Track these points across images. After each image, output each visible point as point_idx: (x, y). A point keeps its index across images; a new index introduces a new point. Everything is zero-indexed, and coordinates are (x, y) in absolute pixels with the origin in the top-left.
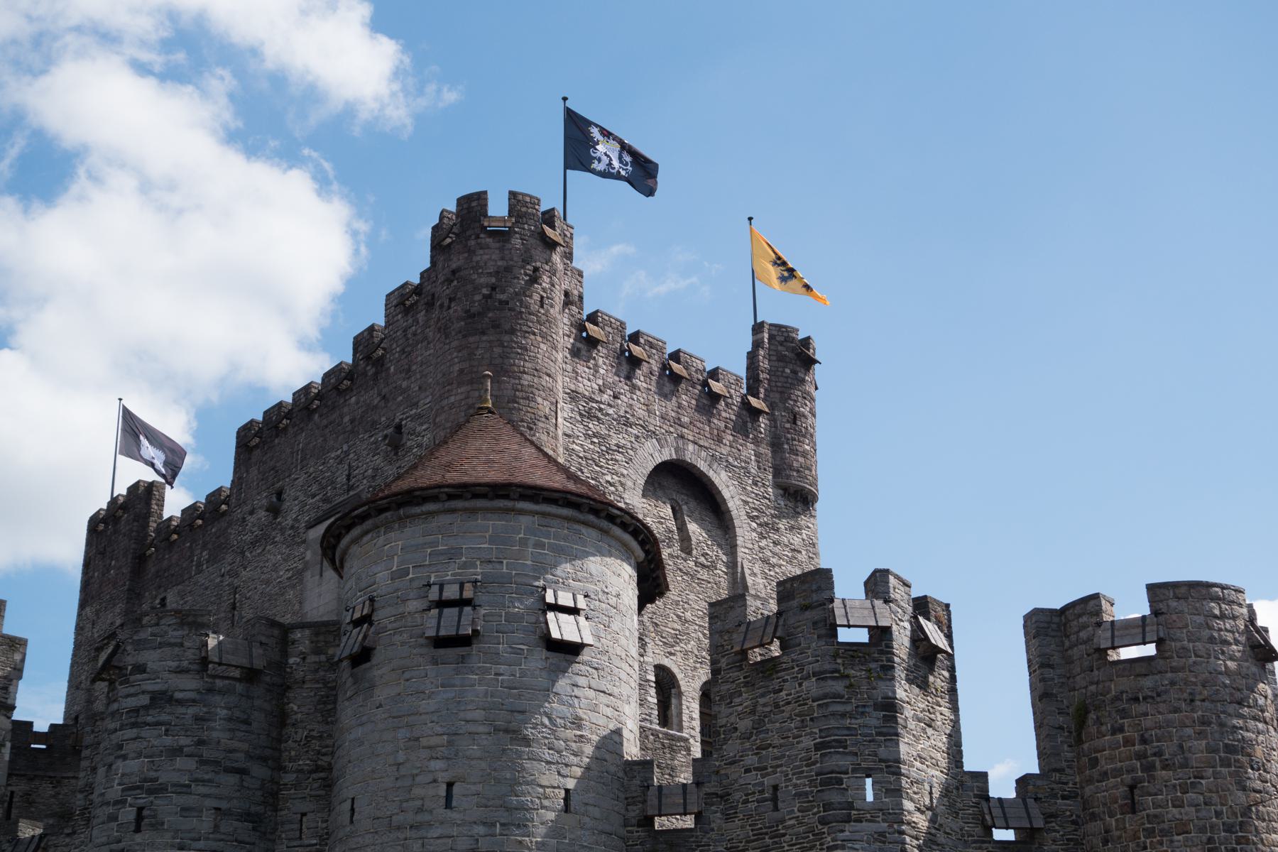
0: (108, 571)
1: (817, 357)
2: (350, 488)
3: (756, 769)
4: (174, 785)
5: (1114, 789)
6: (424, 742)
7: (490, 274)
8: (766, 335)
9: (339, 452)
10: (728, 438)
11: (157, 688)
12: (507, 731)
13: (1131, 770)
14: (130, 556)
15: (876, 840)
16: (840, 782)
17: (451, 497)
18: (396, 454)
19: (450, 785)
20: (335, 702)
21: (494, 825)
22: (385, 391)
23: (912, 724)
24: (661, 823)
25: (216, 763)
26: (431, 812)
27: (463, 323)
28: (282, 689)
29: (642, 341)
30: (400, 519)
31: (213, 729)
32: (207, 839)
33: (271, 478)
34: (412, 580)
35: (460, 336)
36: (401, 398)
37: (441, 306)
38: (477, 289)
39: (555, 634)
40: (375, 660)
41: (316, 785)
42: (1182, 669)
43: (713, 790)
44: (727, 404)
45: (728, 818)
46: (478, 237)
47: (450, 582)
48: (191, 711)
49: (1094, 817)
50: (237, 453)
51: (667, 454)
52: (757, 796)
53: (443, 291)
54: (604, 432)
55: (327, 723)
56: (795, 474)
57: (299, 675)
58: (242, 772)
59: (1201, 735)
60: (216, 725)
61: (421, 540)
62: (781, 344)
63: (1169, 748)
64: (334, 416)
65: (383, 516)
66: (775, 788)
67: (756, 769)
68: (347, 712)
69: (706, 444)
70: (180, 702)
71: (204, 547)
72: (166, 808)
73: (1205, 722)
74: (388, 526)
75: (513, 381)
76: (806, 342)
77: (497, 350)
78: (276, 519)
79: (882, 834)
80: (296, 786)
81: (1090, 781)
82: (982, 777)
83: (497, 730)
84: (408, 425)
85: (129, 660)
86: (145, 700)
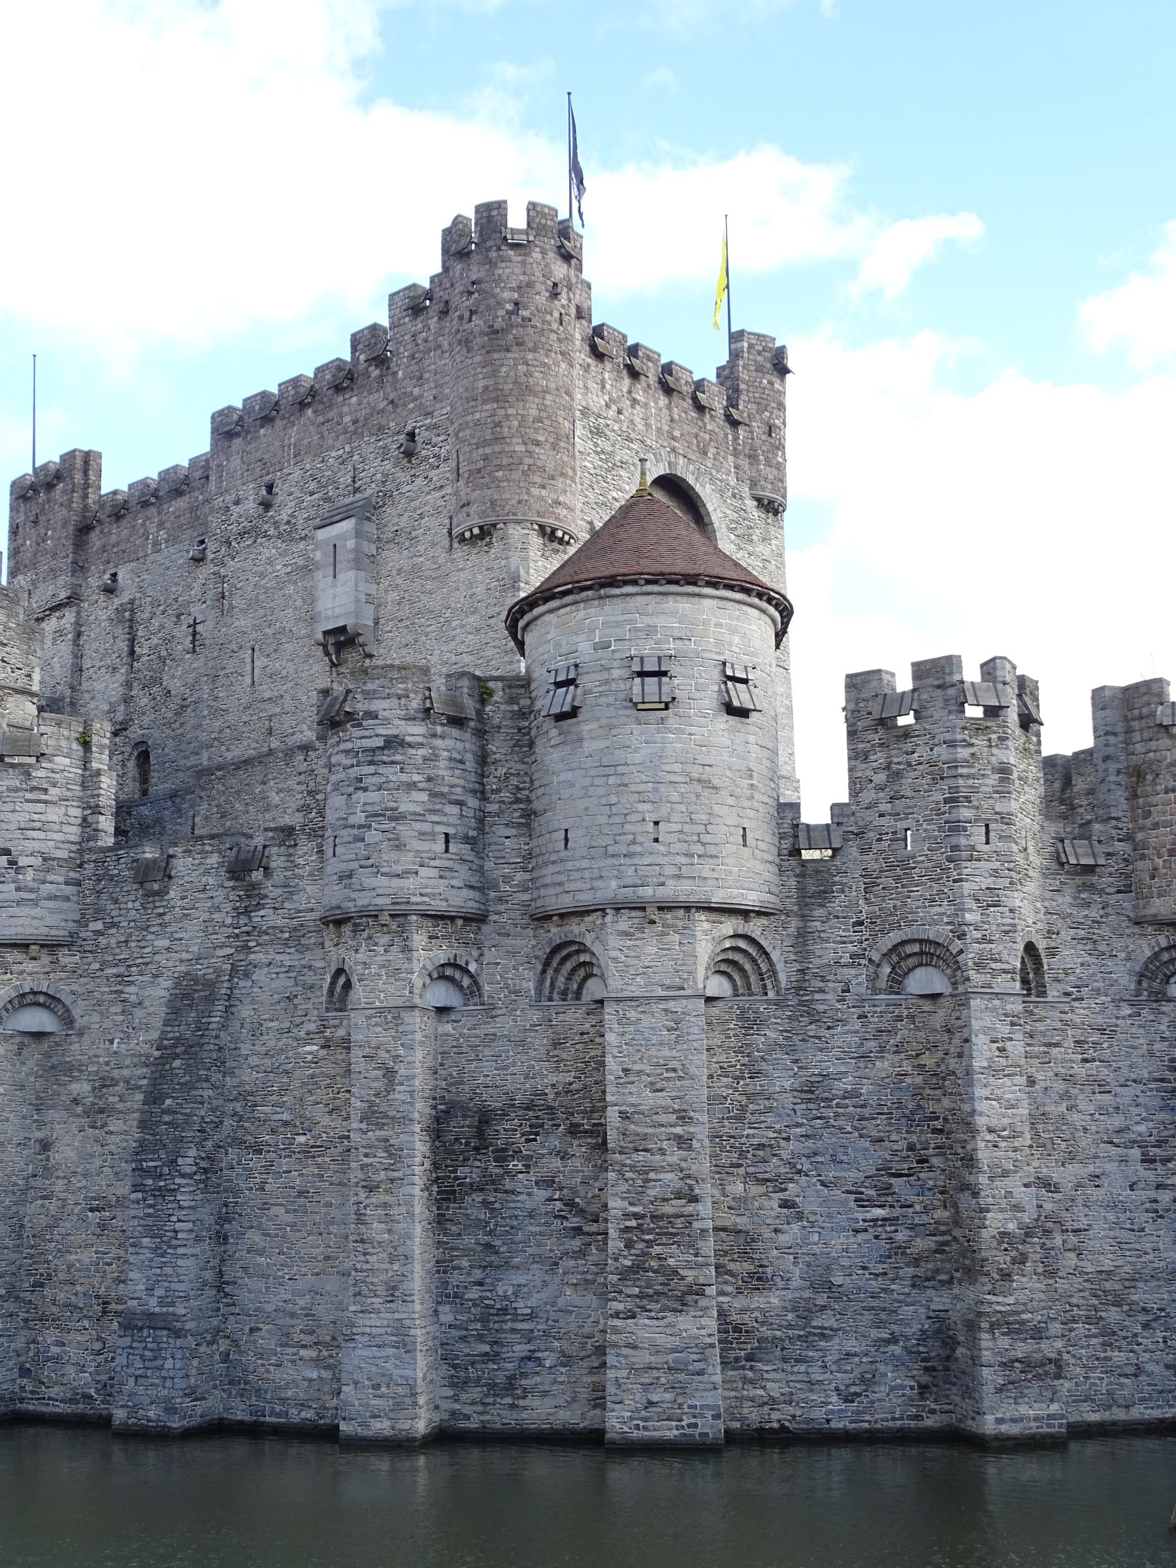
1: (790, 365)
3: (890, 814)
4: (415, 814)
6: (633, 788)
7: (512, 289)
8: (746, 345)
9: (341, 451)
10: (712, 452)
12: (699, 781)
14: (71, 528)
15: (991, 875)
17: (648, 582)
18: (410, 462)
19: (656, 823)
20: (531, 744)
21: (692, 856)
22: (391, 397)
23: (1017, 782)
24: (806, 855)
25: (442, 795)
26: (641, 844)
27: (486, 338)
29: (640, 354)
30: (601, 598)
31: (438, 768)
32: (441, 858)
33: (258, 470)
34: (613, 651)
35: (484, 351)
36: (411, 405)
37: (461, 318)
38: (499, 304)
39: (736, 703)
40: (581, 717)
41: (516, 814)
43: (850, 829)
44: (711, 416)
45: (863, 851)
46: (499, 249)
48: (422, 752)
49: (1143, 857)
50: (212, 438)
51: (661, 470)
52: (890, 836)
54: (610, 449)
55: (523, 763)
56: (769, 486)
57: (496, 721)
58: (460, 803)
60: (442, 764)
61: (621, 618)
62: (759, 353)
65: (584, 594)
67: (890, 814)
69: (694, 458)
70: (410, 745)
71: (161, 525)
72: (406, 831)
75: (537, 401)
77: (522, 368)
78: (268, 511)
79: (995, 871)
81: (1142, 829)
85: (361, 707)
86: (380, 742)
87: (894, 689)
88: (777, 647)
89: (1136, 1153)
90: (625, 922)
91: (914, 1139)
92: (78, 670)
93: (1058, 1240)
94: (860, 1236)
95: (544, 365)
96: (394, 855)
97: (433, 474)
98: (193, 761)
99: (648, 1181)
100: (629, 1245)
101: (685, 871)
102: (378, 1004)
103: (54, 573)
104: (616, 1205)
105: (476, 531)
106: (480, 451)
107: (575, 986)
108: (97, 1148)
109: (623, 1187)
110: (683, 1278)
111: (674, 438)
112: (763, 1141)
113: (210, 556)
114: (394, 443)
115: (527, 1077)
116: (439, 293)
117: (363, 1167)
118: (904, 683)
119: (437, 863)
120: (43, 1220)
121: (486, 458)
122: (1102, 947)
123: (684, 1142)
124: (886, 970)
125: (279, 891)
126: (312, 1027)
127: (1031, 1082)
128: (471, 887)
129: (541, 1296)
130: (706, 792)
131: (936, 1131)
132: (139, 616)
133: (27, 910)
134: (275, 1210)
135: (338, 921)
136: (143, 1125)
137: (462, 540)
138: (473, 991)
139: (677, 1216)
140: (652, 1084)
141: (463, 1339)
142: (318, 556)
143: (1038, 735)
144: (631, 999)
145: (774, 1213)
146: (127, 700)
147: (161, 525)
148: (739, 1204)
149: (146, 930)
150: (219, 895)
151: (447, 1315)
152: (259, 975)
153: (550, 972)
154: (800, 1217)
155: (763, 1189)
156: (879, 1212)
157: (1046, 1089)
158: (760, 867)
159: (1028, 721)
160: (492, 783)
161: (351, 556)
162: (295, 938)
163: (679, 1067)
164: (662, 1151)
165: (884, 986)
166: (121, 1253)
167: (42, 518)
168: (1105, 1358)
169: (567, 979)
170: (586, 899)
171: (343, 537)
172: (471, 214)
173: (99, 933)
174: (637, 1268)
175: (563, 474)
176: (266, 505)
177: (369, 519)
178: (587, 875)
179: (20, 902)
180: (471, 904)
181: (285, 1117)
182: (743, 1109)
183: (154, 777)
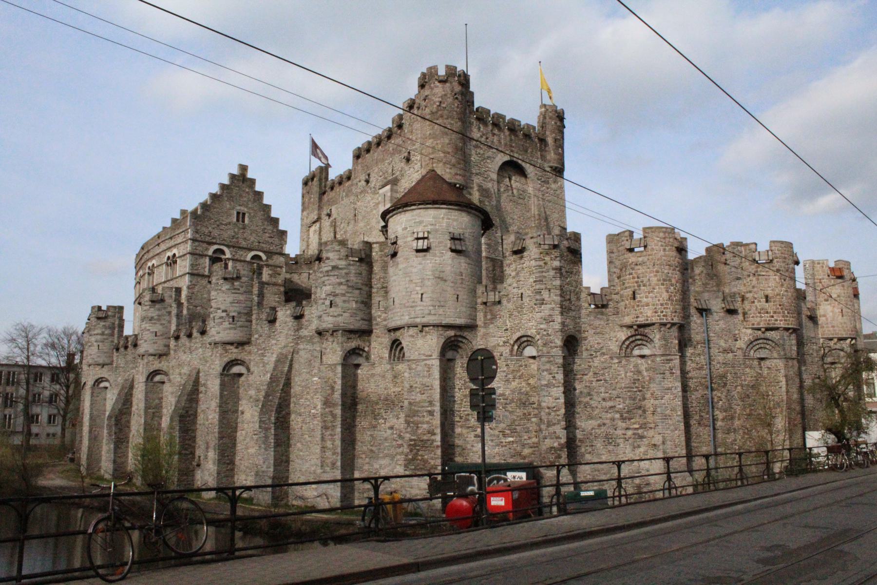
0: (311, 198)
2: (393, 174)
5: (629, 292)
6: (414, 281)
10: (529, 151)
12: (439, 278)
13: (634, 286)
17: (419, 204)
19: (422, 294)
25: (352, 287)
30: (405, 211)
38: (435, 103)
39: (453, 248)
40: (399, 255)
42: (652, 255)
45: (508, 302)
48: (345, 271)
49: (623, 300)
53: (423, 103)
58: (360, 289)
59: (656, 276)
63: (645, 280)
66: (522, 294)
68: (391, 270)
70: (341, 269)
71: (344, 191)
72: (339, 300)
73: (657, 272)
74: (400, 212)
79: (553, 308)
82: (589, 288)
83: (436, 278)
84: (412, 153)
85: (324, 255)
86: (330, 268)
89: (617, 416)
90: (412, 331)
91: (526, 411)
93: (583, 450)
94: (503, 448)
97: (416, 167)
99: (418, 427)
100: (411, 451)
101: (433, 312)
103: (313, 210)
109: (409, 429)
111: (511, 146)
115: (385, 389)
116: (417, 101)
117: (325, 421)
123: (431, 413)
124: (516, 347)
125: (307, 323)
126: (316, 371)
130: (442, 283)
132: (338, 224)
133: (232, 331)
135: (320, 333)
138: (368, 358)
139: (428, 440)
147: (344, 191)
149: (270, 337)
150: (291, 323)
152: (302, 353)
155: (468, 430)
156: (511, 439)
157: (581, 392)
158: (464, 309)
160: (374, 281)
163: (429, 384)
164: (424, 416)
165: (515, 353)
169: (400, 352)
170: (399, 323)
171: (386, 192)
173: (257, 339)
174: (413, 459)
176: (367, 182)
177: (396, 185)
178: (399, 314)
179: (230, 329)
181: (308, 403)
182: (462, 400)
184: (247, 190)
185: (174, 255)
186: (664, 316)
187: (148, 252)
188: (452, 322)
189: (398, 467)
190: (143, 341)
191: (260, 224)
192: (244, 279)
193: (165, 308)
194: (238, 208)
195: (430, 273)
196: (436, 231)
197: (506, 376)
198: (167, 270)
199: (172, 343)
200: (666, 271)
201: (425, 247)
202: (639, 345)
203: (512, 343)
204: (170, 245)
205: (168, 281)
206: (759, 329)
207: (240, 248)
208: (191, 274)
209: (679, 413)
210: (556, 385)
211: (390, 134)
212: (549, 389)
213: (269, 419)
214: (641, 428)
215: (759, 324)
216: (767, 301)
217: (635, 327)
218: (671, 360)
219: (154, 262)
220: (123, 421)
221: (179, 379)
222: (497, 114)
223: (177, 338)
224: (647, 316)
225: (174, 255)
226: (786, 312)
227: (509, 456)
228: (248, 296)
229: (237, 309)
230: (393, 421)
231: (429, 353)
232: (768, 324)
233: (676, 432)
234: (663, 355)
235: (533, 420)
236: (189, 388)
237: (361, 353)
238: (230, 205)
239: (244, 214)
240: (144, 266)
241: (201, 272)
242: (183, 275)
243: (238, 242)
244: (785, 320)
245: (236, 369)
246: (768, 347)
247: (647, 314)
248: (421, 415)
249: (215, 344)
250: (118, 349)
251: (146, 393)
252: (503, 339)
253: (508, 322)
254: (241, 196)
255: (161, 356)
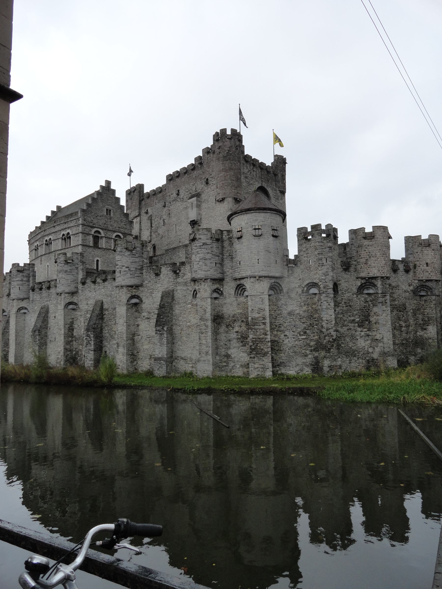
1: (287, 162)
2: (196, 191)
5: (363, 260)
11: (204, 242)
16: (322, 260)
17: (256, 210)
19: (258, 260)
20: (233, 244)
25: (215, 255)
28: (223, 241)
30: (246, 213)
37: (217, 154)
38: (225, 151)
39: (274, 235)
40: (243, 238)
45: (301, 265)
47: (257, 225)
48: (210, 246)
49: (359, 265)
51: (260, 185)
53: (217, 151)
58: (218, 256)
59: (379, 252)
63: (373, 254)
64: (191, 175)
65: (243, 213)
70: (207, 245)
71: (157, 199)
73: (380, 250)
76: (285, 159)
80: (226, 258)
81: (359, 259)
84: (209, 179)
85: (198, 236)
87: (307, 231)
88: (283, 222)
89: (357, 325)
90: (252, 280)
92: (141, 230)
94: (300, 342)
95: (235, 164)
96: (205, 267)
98: (164, 248)
100: (253, 344)
101: (264, 269)
102: (203, 297)
103: (135, 210)
104: (251, 336)
105: (221, 199)
106: (222, 182)
107: (242, 293)
108: (148, 326)
110: (264, 350)
111: (262, 179)
112: (281, 323)
113: (167, 206)
114: (204, 181)
117: (200, 329)
118: (309, 230)
119: (214, 268)
120: (138, 340)
121: (223, 184)
122: (351, 283)
123: (264, 324)
124: (305, 289)
125: (182, 275)
126: (190, 302)
127: (335, 311)
128: (221, 273)
129: (236, 354)
131: (315, 321)
133: (133, 279)
134: (183, 338)
135: (194, 280)
136: (157, 321)
137: (218, 201)
138: (222, 294)
140: (258, 312)
141: (221, 362)
142: (189, 205)
143: (337, 240)
144: (254, 295)
145: (283, 337)
146: (151, 236)
147: (157, 199)
148: (275, 336)
151: (218, 358)
152: (179, 291)
153: (237, 290)
154: (288, 338)
155: (281, 333)
156: (304, 337)
157: (338, 312)
159: (336, 238)
161: (196, 205)
162: (186, 284)
164: (260, 325)
165: (305, 291)
166: (154, 346)
167: (132, 199)
168: (350, 365)
169: (241, 291)
170: (244, 275)
172: (219, 131)
175: (239, 187)
176: (178, 194)
177: (199, 197)
179: (131, 278)
180: (221, 277)
181: (185, 319)
182: (276, 317)
183: (157, 251)
184: (111, 196)
185: (68, 233)
186: (383, 273)
187: (45, 231)
188: (274, 275)
189: (242, 353)
190: (61, 285)
191: (119, 217)
192: (138, 249)
193: (74, 265)
194: (107, 206)
195: (262, 248)
196: (265, 225)
197: (300, 304)
198: (62, 243)
199: (80, 286)
200: (384, 250)
201: (260, 234)
202: (367, 288)
203: (303, 286)
204: (64, 227)
205: (67, 248)
206: (422, 280)
207: (109, 230)
208: (83, 245)
209: (390, 323)
210: (330, 309)
211: (193, 168)
212: (327, 311)
213: (163, 328)
214: (368, 331)
215: (422, 278)
216: (427, 266)
217: (367, 279)
218: (386, 296)
219: (50, 237)
220: (43, 333)
221: (87, 307)
222: (254, 159)
223: (84, 283)
224: (374, 273)
225: (68, 233)
226: (436, 271)
227: (303, 346)
228: (141, 259)
229: (136, 266)
230: (237, 329)
231: (263, 292)
232: (428, 278)
233: (388, 333)
234: (381, 293)
235: (315, 327)
236: (97, 312)
237: (218, 291)
238: (102, 204)
239: (110, 210)
240: (41, 239)
241: (88, 244)
242: (77, 246)
243: (107, 227)
244: (436, 276)
245: (134, 301)
246: (425, 289)
247: (374, 272)
248: (258, 325)
249: (121, 286)
250: (33, 290)
251: (65, 315)
252: (298, 284)
253: (300, 275)
254: (108, 200)
255: (73, 293)
